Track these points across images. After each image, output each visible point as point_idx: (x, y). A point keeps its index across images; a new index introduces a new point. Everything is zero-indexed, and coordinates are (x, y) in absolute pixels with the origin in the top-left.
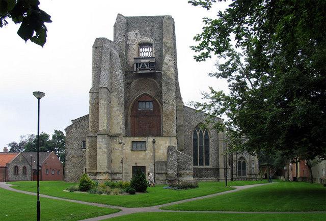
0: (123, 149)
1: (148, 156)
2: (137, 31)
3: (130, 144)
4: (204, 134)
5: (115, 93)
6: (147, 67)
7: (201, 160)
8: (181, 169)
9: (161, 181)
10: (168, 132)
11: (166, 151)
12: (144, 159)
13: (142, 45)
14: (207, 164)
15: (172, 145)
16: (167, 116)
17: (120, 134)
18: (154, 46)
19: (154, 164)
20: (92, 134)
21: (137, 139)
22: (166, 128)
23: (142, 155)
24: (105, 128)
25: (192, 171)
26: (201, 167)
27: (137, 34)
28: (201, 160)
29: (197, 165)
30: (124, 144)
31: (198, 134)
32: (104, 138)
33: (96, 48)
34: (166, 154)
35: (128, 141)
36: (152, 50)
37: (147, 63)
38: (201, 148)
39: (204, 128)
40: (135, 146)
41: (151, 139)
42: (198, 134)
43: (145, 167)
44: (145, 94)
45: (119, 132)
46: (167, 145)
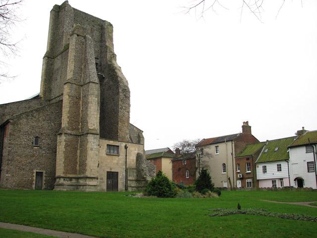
1: (120, 162)
3: (106, 147)
9: (133, 188)
12: (117, 164)
15: (140, 152)
20: (69, 132)
22: (121, 134)
23: (115, 160)
34: (135, 161)
40: (112, 151)
41: (124, 144)
43: (118, 173)
46: (136, 152)
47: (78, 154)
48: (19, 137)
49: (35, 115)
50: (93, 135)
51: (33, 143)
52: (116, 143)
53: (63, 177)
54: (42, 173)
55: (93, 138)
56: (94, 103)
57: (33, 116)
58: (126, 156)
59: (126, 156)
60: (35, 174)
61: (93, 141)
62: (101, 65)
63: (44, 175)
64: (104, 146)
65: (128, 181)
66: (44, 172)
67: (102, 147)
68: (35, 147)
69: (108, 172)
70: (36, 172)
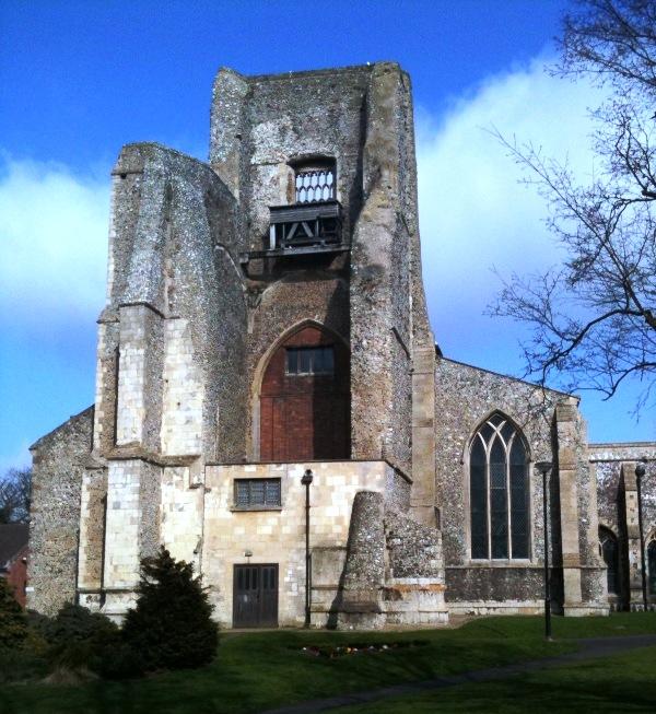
0: (202, 505)
1: (287, 530)
2: (286, 121)
3: (228, 488)
4: (508, 448)
5: (183, 323)
6: (310, 234)
7: (500, 540)
8: (400, 572)
10: (369, 442)
11: (346, 512)
12: (273, 537)
13: (299, 165)
14: (522, 550)
16: (366, 393)
17: (194, 458)
18: (339, 167)
19: (308, 557)
21: (250, 471)
22: (359, 431)
23: (266, 523)
24: (138, 436)
25: (439, 580)
26: (500, 563)
27: (283, 131)
28: (500, 540)
29: (486, 557)
30: (207, 490)
31: (488, 449)
32: (132, 471)
33: (123, 176)
35: (225, 478)
36: (335, 179)
37: (311, 224)
38: (499, 496)
39: (510, 427)
41: (298, 471)
42: (488, 449)
43: (276, 565)
44: (311, 324)
45: (193, 451)
48: (50, 491)
50: (122, 464)
52: (272, 471)
53: (85, 592)
56: (134, 365)
57: (79, 432)
58: (308, 507)
59: (308, 507)
61: (121, 480)
64: (221, 485)
65: (315, 594)
67: (215, 489)
69: (237, 567)
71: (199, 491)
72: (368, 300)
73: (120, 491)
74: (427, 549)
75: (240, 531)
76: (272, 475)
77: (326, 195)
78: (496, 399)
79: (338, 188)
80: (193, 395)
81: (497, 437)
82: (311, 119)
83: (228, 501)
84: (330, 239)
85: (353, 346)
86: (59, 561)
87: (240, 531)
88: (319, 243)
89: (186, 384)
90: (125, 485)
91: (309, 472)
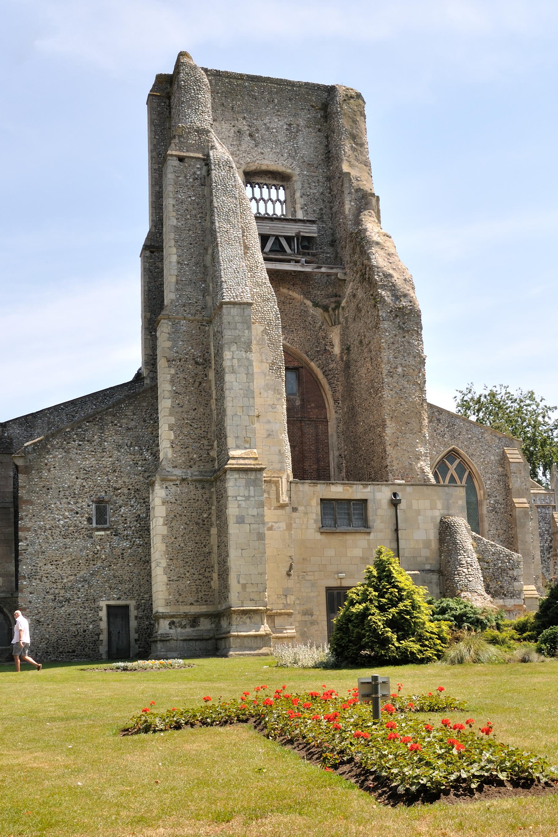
2: (243, 126)
11: (432, 535)
18: (298, 185)
30: (295, 510)
34: (434, 545)
46: (437, 514)
47: (214, 540)
48: (46, 507)
49: (89, 435)
51: (89, 520)
54: (127, 607)
55: (242, 482)
57: (83, 440)
59: (397, 530)
60: (103, 614)
61: (243, 491)
62: (333, 243)
63: (133, 613)
64: (308, 505)
66: (132, 604)
67: (301, 509)
68: (98, 530)
70: (108, 607)
71: (288, 509)
72: (400, 328)
73: (243, 504)
74: (510, 572)
75: (330, 552)
76: (359, 496)
77: (279, 210)
78: (453, 437)
79: (298, 206)
80: (273, 406)
81: (452, 475)
82: (268, 129)
83: (316, 521)
84: (309, 258)
85: (385, 372)
86: (64, 588)
87: (330, 552)
88: (297, 262)
89: (265, 394)
90: (247, 498)
91: (395, 495)
